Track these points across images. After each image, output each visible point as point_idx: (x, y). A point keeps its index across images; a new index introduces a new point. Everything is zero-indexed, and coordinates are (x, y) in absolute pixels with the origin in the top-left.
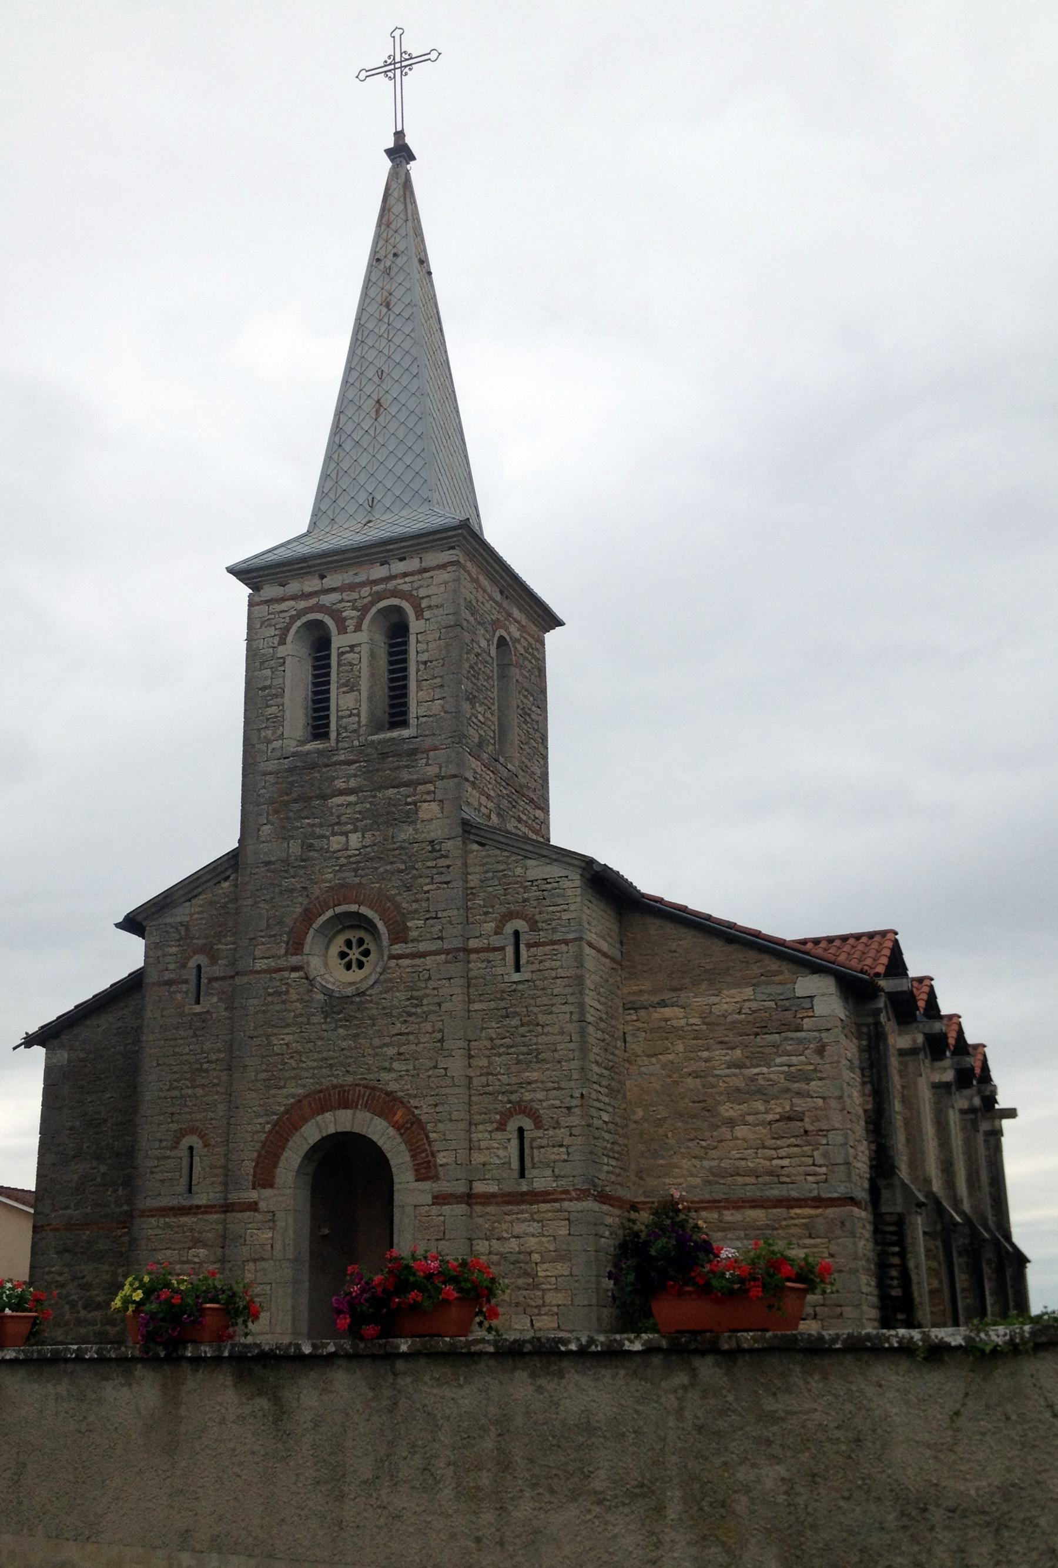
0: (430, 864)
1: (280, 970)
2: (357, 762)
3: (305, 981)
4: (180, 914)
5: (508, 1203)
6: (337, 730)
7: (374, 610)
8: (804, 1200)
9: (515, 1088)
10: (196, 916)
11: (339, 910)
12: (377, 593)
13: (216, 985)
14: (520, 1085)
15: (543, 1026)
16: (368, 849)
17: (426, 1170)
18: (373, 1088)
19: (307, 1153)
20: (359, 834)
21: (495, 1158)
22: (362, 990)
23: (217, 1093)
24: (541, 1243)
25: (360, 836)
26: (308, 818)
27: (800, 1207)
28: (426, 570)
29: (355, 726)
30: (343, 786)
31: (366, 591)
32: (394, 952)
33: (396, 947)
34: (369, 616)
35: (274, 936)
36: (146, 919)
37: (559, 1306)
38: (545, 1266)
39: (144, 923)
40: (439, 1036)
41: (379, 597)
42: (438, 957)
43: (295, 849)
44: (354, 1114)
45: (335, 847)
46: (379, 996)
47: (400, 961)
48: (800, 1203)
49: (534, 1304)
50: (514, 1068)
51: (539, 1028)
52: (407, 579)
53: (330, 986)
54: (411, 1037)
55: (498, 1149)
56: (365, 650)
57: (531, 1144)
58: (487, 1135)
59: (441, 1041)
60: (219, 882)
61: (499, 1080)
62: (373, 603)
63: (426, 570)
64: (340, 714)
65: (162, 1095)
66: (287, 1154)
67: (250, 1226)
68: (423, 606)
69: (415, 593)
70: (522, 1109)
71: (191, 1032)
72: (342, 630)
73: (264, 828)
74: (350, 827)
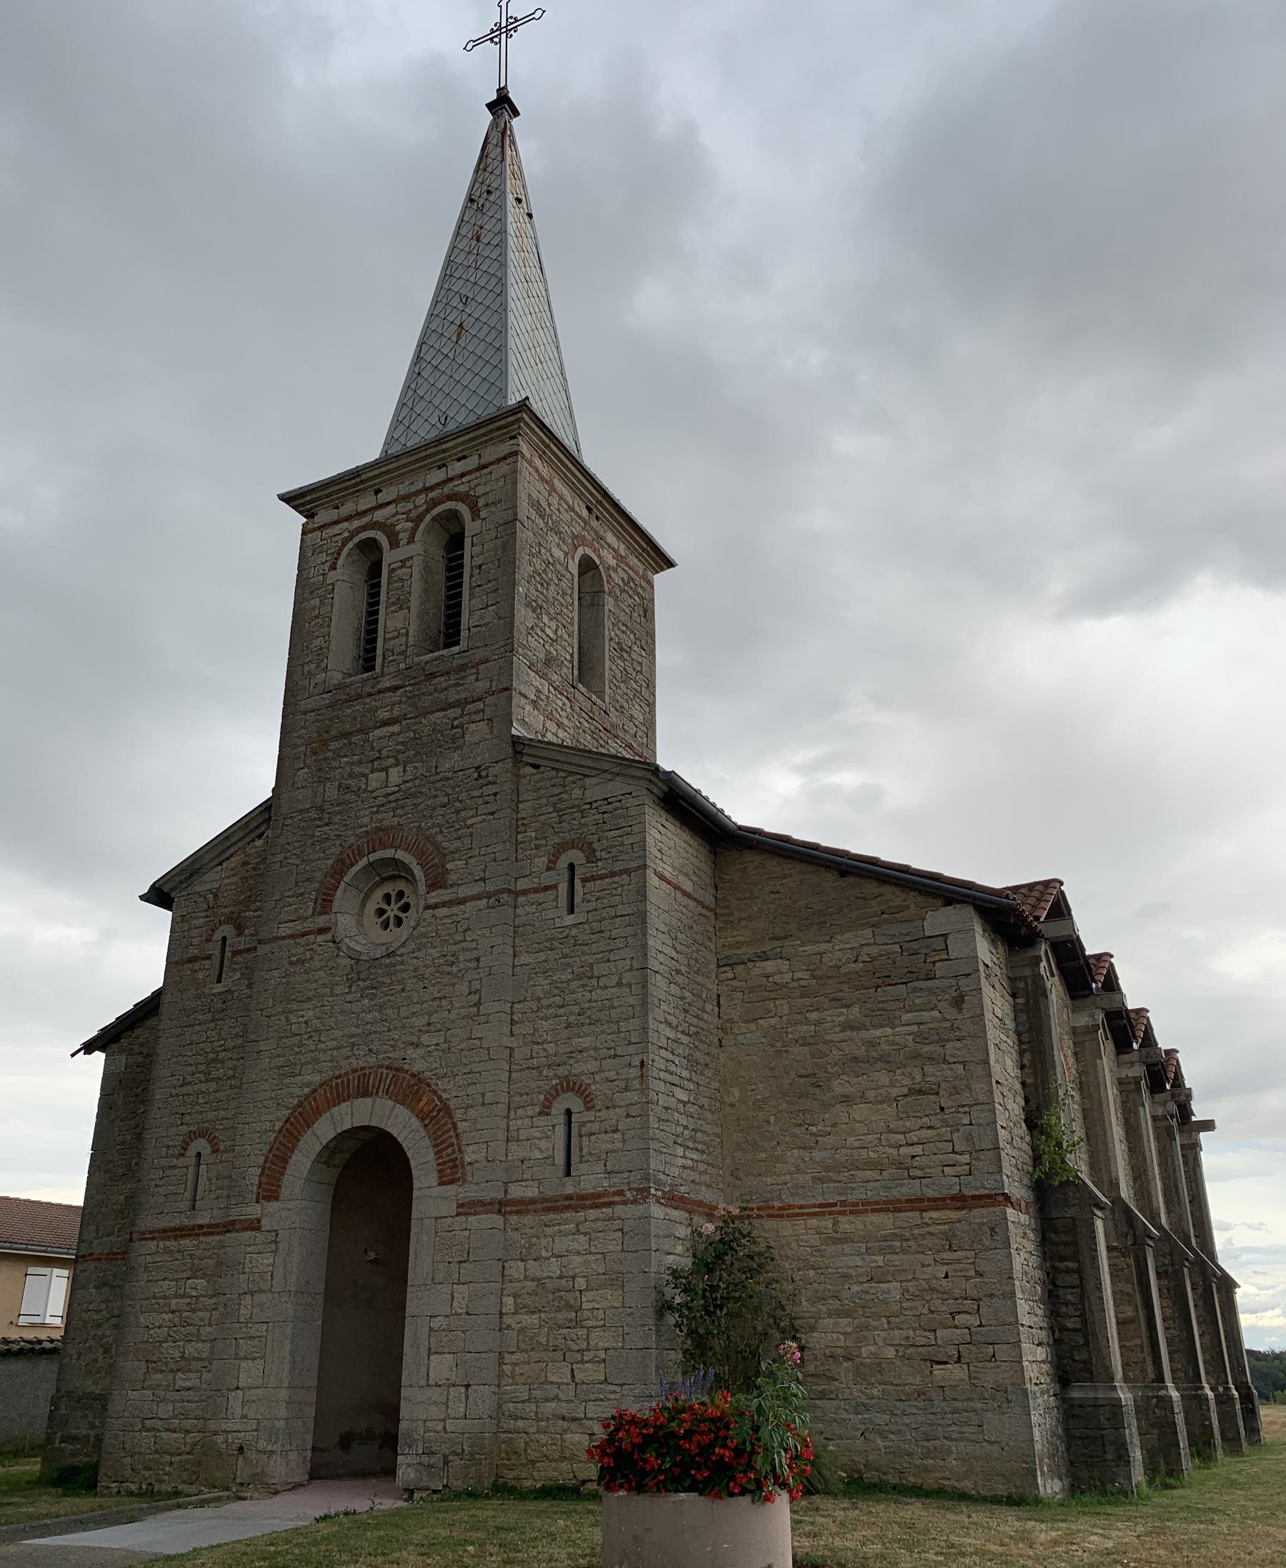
0: (475, 793)
1: (304, 934)
2: (402, 687)
3: (331, 944)
4: (210, 881)
5: (548, 1210)
6: (384, 654)
7: (428, 518)
8: (943, 1199)
9: (564, 1058)
10: (228, 881)
11: (373, 857)
12: (433, 499)
13: (238, 959)
14: (570, 1055)
15: (598, 978)
16: (410, 784)
17: (451, 1172)
18: (397, 1070)
19: (320, 1155)
20: (400, 768)
21: (536, 1151)
22: (392, 949)
23: (231, 1087)
24: (586, 1263)
25: (401, 770)
26: (346, 756)
27: (937, 1209)
28: (484, 467)
29: (403, 647)
30: (387, 715)
31: (421, 499)
32: (432, 901)
33: (433, 894)
34: (422, 526)
35: (302, 894)
36: (173, 889)
37: (606, 1349)
38: (590, 1295)
39: (173, 895)
40: (475, 998)
41: (435, 503)
42: (478, 902)
43: (331, 792)
44: (374, 1102)
45: (373, 785)
46: (412, 955)
47: (436, 911)
48: (938, 1203)
49: (575, 1347)
50: (564, 1034)
51: (594, 982)
52: (464, 480)
53: (358, 948)
54: (444, 1003)
55: (539, 1139)
56: (417, 564)
57: (580, 1130)
58: (527, 1121)
59: (478, 1004)
60: (253, 840)
61: (545, 1050)
62: (427, 511)
63: (484, 467)
64: (387, 636)
65: (174, 1091)
66: (296, 1157)
67: (249, 1249)
68: (480, 505)
69: (472, 493)
70: (570, 1085)
71: (210, 1016)
72: (394, 544)
73: (301, 772)
74: (391, 761)
